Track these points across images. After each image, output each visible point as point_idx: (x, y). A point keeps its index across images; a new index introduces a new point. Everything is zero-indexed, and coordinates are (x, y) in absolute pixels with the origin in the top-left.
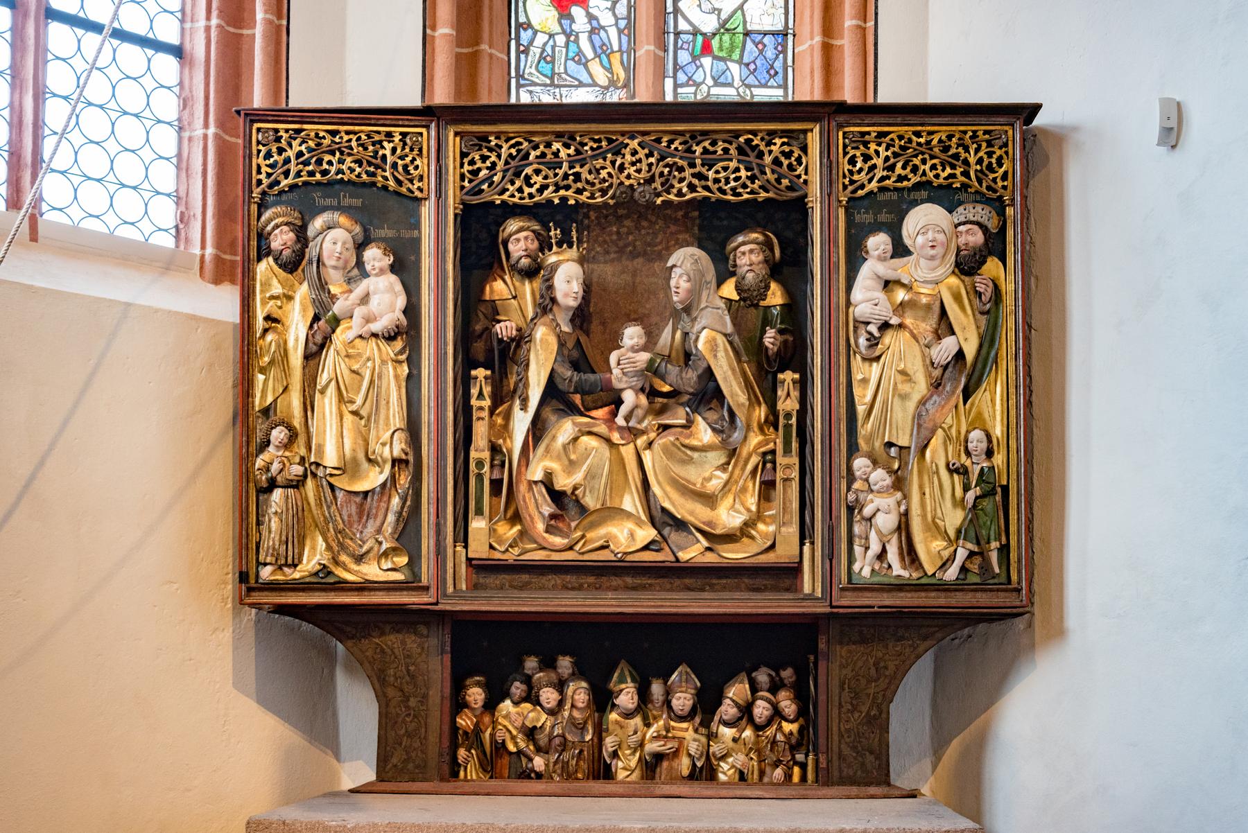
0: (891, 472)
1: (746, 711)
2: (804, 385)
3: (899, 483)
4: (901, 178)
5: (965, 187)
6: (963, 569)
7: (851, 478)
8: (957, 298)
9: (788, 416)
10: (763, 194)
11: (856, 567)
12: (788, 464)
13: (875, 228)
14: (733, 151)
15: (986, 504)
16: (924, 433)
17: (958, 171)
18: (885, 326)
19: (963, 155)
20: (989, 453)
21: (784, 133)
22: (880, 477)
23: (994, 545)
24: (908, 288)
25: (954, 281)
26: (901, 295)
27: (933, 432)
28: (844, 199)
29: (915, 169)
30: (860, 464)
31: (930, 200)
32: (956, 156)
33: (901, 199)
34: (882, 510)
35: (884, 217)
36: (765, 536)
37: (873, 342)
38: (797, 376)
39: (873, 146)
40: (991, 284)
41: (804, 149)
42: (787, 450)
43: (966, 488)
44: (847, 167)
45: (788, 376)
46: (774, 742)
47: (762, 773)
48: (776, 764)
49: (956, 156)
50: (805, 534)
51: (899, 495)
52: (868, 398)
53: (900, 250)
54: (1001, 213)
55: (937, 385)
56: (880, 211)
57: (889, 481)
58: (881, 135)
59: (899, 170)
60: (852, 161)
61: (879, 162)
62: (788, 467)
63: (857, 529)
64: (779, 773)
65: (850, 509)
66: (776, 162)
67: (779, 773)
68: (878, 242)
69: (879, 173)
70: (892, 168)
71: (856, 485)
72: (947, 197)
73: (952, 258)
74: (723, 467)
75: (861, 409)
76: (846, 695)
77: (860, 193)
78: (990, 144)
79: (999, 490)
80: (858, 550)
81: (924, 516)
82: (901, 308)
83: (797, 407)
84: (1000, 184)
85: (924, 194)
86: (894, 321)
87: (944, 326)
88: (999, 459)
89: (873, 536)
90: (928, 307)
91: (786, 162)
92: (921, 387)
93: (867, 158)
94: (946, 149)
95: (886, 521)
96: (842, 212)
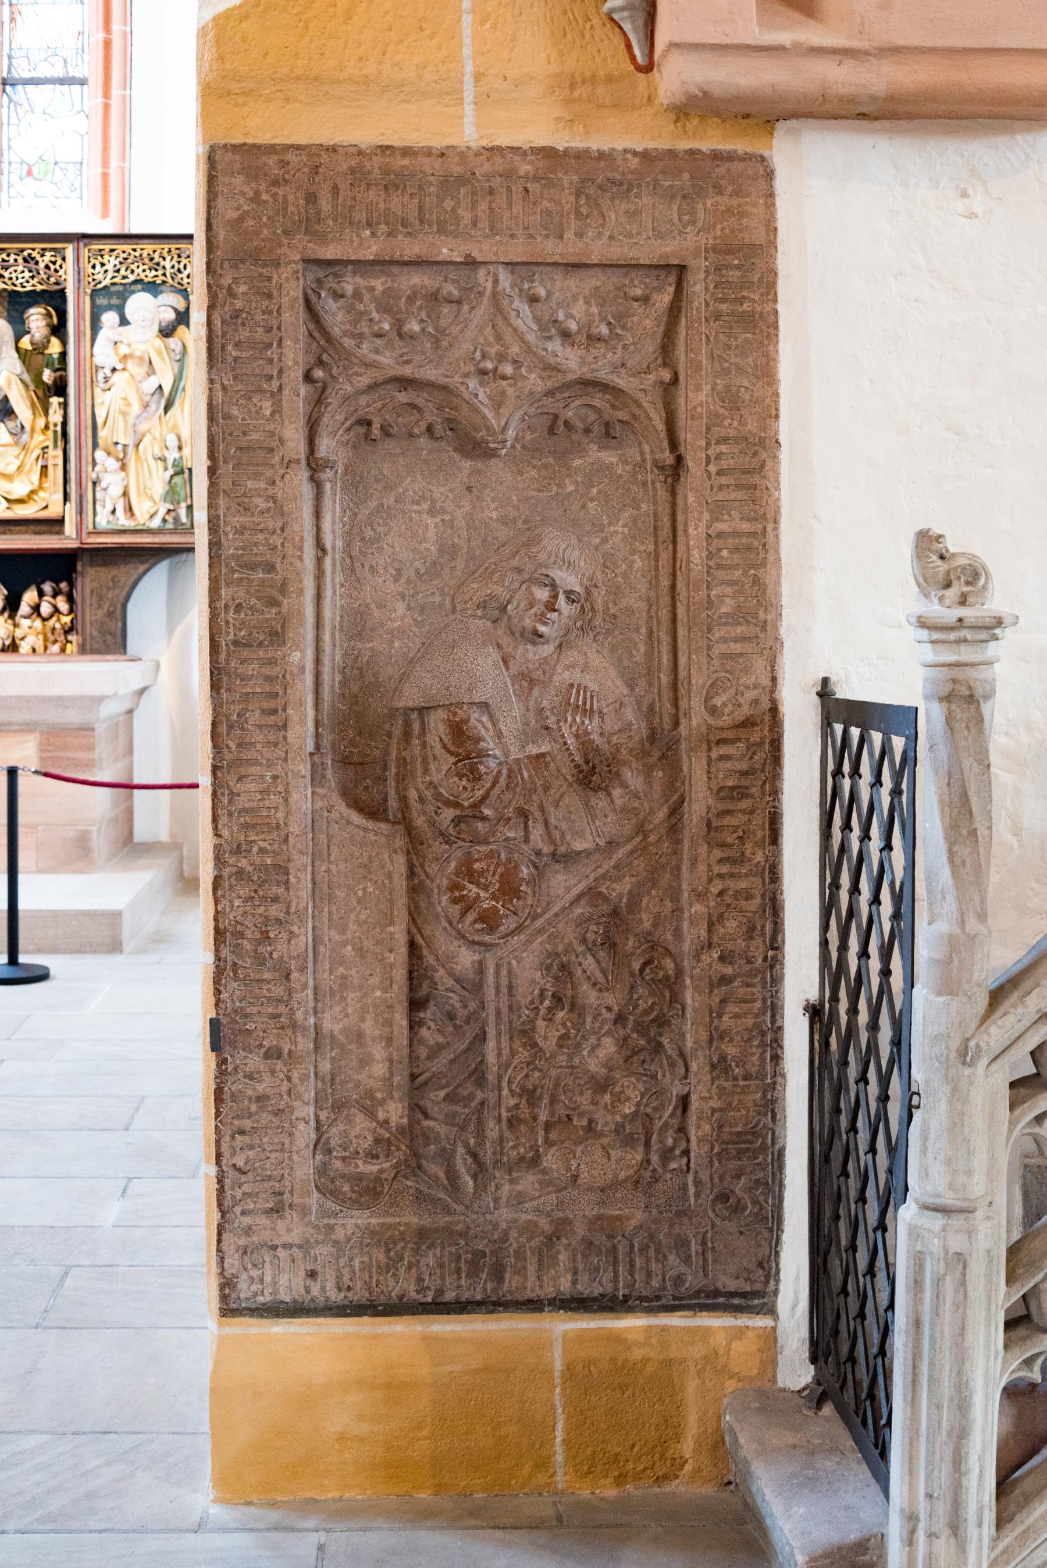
0: (118, 459)
1: (36, 609)
2: (65, 406)
3: (123, 467)
4: (124, 277)
5: (164, 282)
6: (164, 520)
7: (94, 463)
8: (159, 353)
9: (55, 425)
10: (39, 288)
11: (98, 519)
12: (55, 456)
13: (110, 307)
14: (20, 260)
15: (178, 479)
16: (139, 437)
17: (160, 272)
18: (114, 370)
19: (162, 263)
20: (180, 448)
21: (52, 250)
22: (112, 464)
23: (183, 505)
24: (129, 346)
25: (158, 342)
26: (124, 350)
27: (143, 435)
28: (89, 291)
29: (132, 272)
30: (99, 454)
31: (143, 290)
32: (158, 264)
33: (125, 290)
34: (112, 482)
35: (115, 301)
36: (43, 499)
37: (106, 379)
38: (62, 400)
39: (106, 257)
40: (180, 344)
41: (64, 259)
42: (55, 446)
43: (166, 469)
44: (91, 271)
45: (55, 401)
46: (54, 629)
47: (46, 648)
48: (55, 642)
49: (158, 264)
50: (66, 498)
51: (123, 474)
52: (104, 415)
53: (124, 322)
54: (186, 298)
55: (146, 406)
56: (111, 298)
57: (117, 465)
58: (112, 250)
59: (123, 272)
60: (94, 267)
61: (109, 267)
62: (55, 457)
63: (98, 495)
64: (56, 648)
65: (94, 483)
66: (47, 267)
67: (56, 648)
68: (109, 318)
69: (110, 274)
70: (118, 271)
71: (97, 468)
72: (153, 288)
73: (156, 328)
74: (17, 457)
75: (100, 421)
76: (95, 599)
77: (99, 286)
78: (179, 256)
79: (187, 471)
80: (98, 508)
81: (138, 488)
82: (125, 358)
83: (61, 419)
84: (186, 281)
85: (139, 287)
86: (119, 366)
87: (151, 370)
88: (186, 451)
89: (108, 500)
90: (141, 358)
91: (52, 267)
92: (136, 408)
93: (103, 265)
94: (152, 259)
95: (116, 491)
96: (88, 299)
